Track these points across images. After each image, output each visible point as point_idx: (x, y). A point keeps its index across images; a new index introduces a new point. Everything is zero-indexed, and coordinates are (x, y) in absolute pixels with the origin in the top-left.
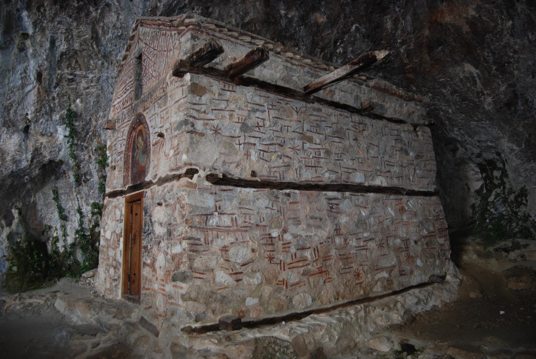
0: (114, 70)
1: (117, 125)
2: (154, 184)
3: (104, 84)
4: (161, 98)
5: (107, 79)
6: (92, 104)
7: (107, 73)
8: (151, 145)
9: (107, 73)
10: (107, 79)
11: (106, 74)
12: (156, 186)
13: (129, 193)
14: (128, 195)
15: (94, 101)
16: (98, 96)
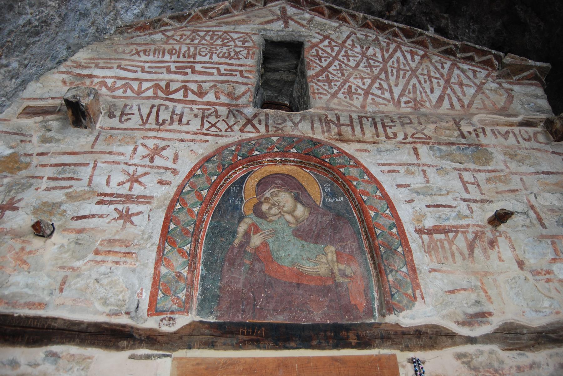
0: (106, 14)
1: (102, 122)
2: (471, 340)
3: (72, 15)
4: (453, 144)
5: (84, 15)
6: (21, 22)
7: (94, 6)
8: (409, 229)
9: (94, 6)
10: (84, 15)
11: (89, 5)
12: (494, 347)
13: (211, 345)
14: (181, 353)
15: (30, 22)
16: (45, 23)
